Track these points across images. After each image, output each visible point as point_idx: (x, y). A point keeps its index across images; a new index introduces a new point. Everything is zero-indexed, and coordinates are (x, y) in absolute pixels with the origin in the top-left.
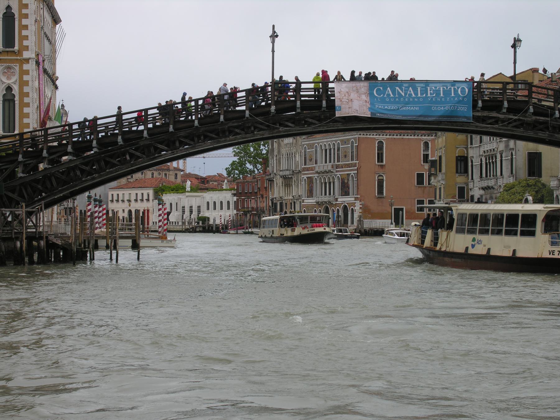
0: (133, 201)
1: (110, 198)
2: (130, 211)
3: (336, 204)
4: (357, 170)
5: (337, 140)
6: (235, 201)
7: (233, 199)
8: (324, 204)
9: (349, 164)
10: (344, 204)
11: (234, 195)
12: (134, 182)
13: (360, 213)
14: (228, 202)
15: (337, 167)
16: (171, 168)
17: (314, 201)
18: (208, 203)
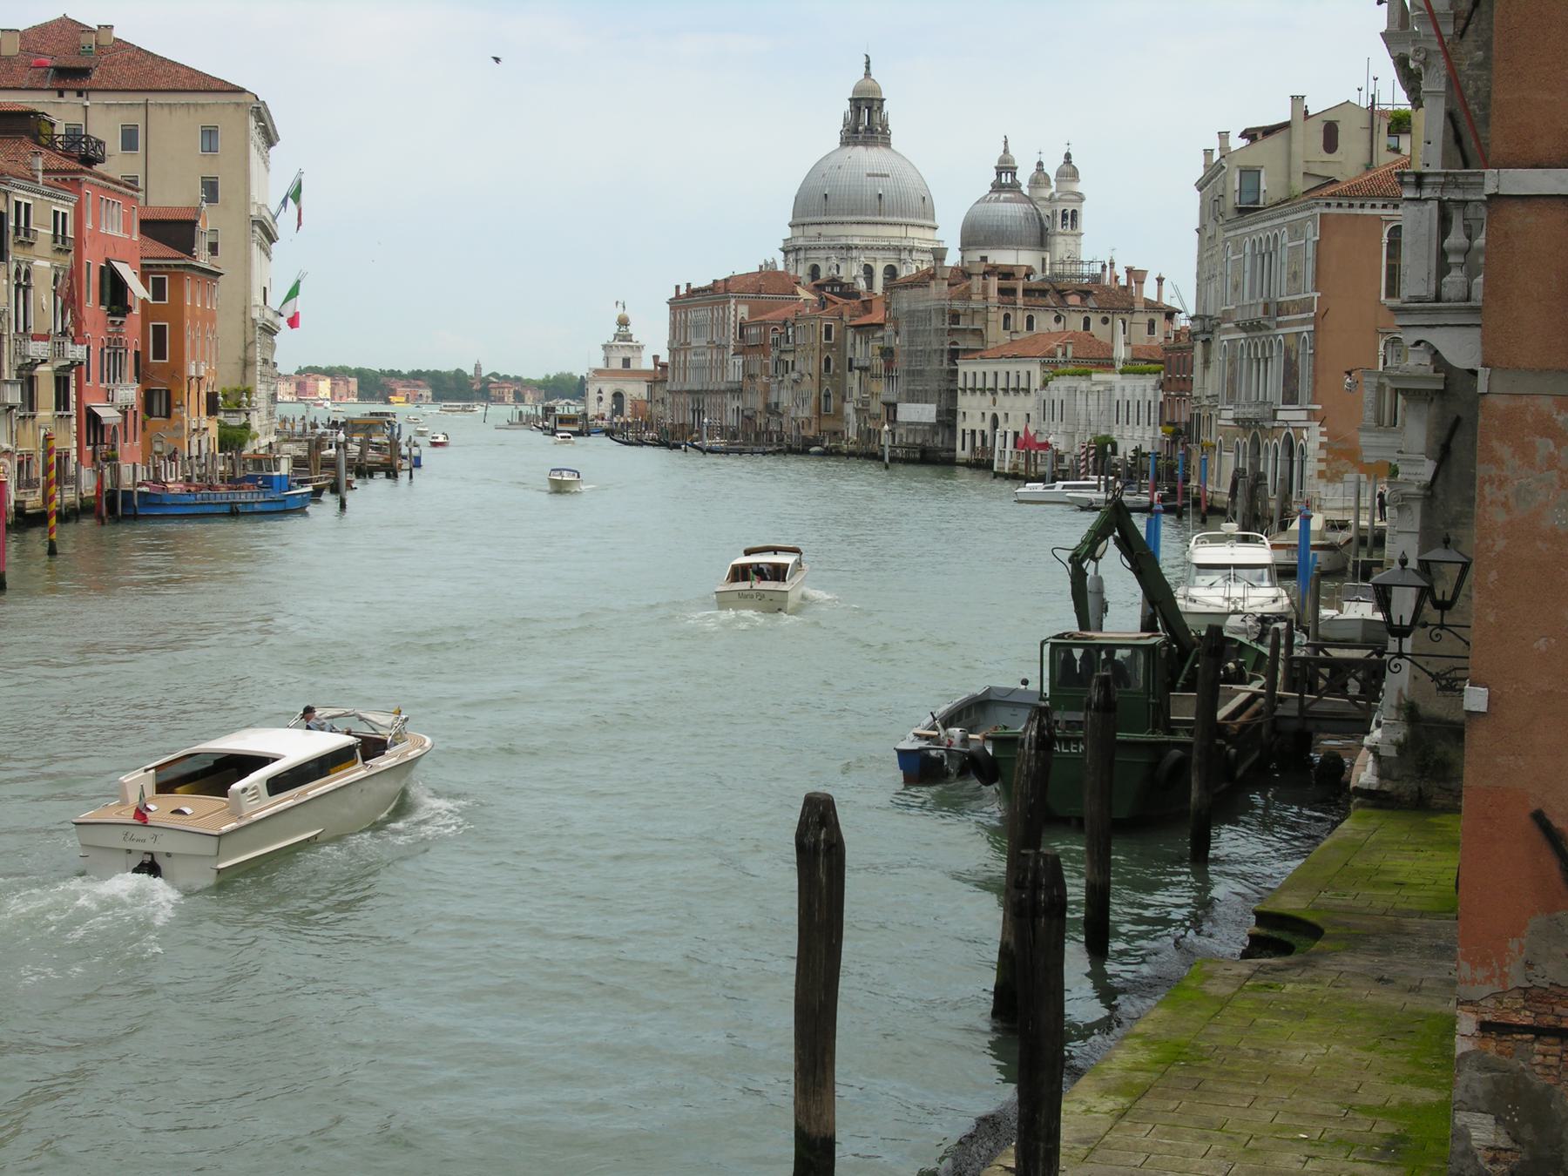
0: (1000, 392)
1: (961, 384)
2: (995, 417)
3: (1273, 427)
4: (1315, 321)
5: (1279, 226)
6: (1161, 403)
7: (1156, 396)
8: (1250, 429)
9: (1301, 300)
10: (1286, 430)
11: (1162, 386)
12: (1021, 340)
13: (1320, 460)
14: (1150, 402)
15: (1281, 309)
16: (1139, 306)
17: (1230, 414)
18: (1118, 402)
